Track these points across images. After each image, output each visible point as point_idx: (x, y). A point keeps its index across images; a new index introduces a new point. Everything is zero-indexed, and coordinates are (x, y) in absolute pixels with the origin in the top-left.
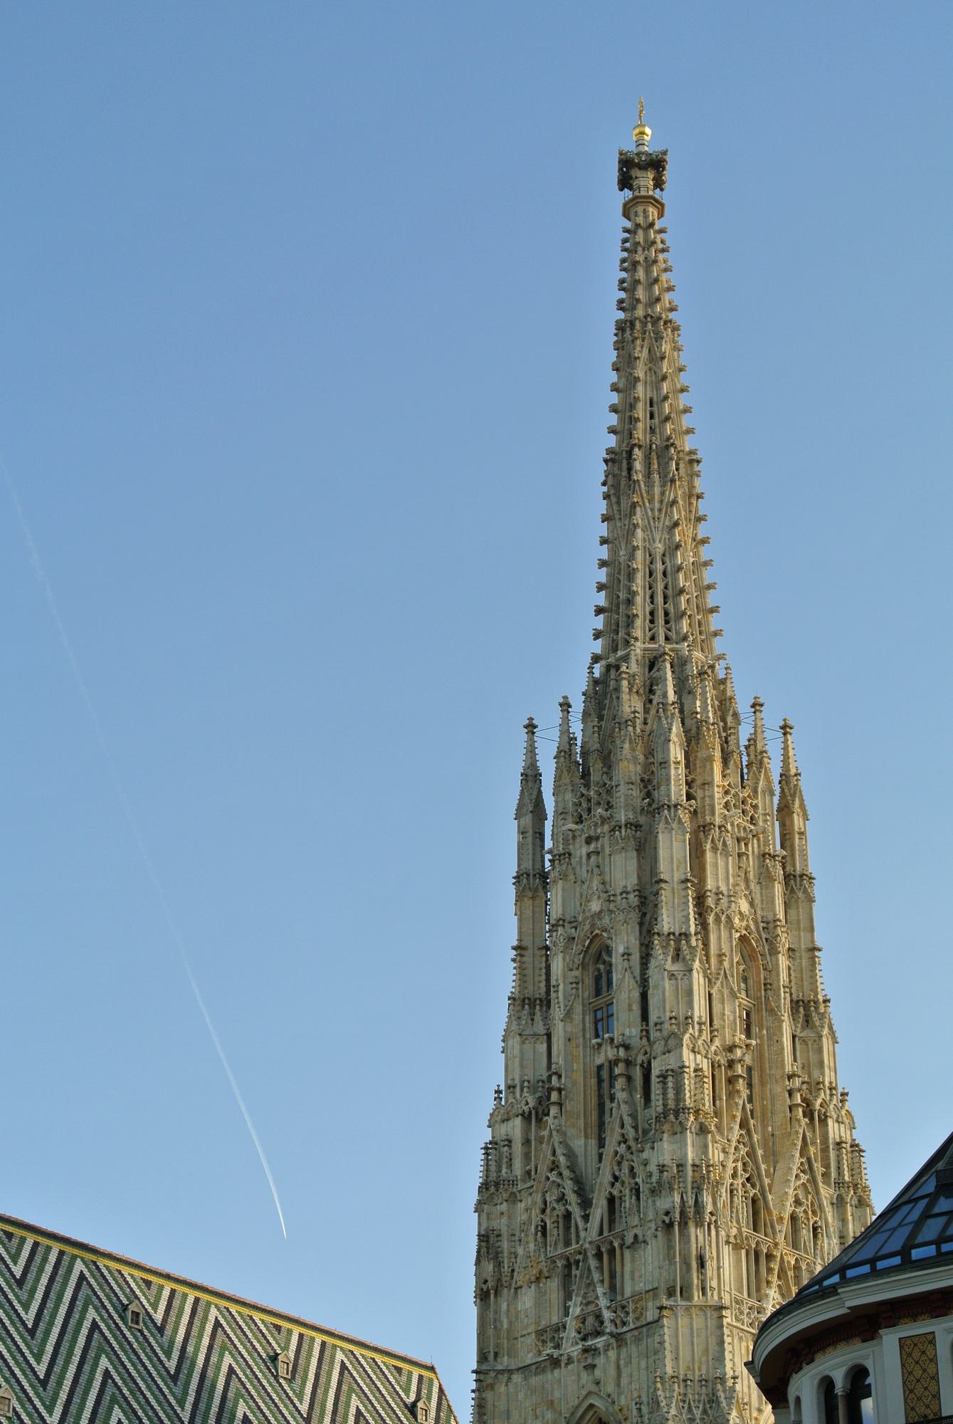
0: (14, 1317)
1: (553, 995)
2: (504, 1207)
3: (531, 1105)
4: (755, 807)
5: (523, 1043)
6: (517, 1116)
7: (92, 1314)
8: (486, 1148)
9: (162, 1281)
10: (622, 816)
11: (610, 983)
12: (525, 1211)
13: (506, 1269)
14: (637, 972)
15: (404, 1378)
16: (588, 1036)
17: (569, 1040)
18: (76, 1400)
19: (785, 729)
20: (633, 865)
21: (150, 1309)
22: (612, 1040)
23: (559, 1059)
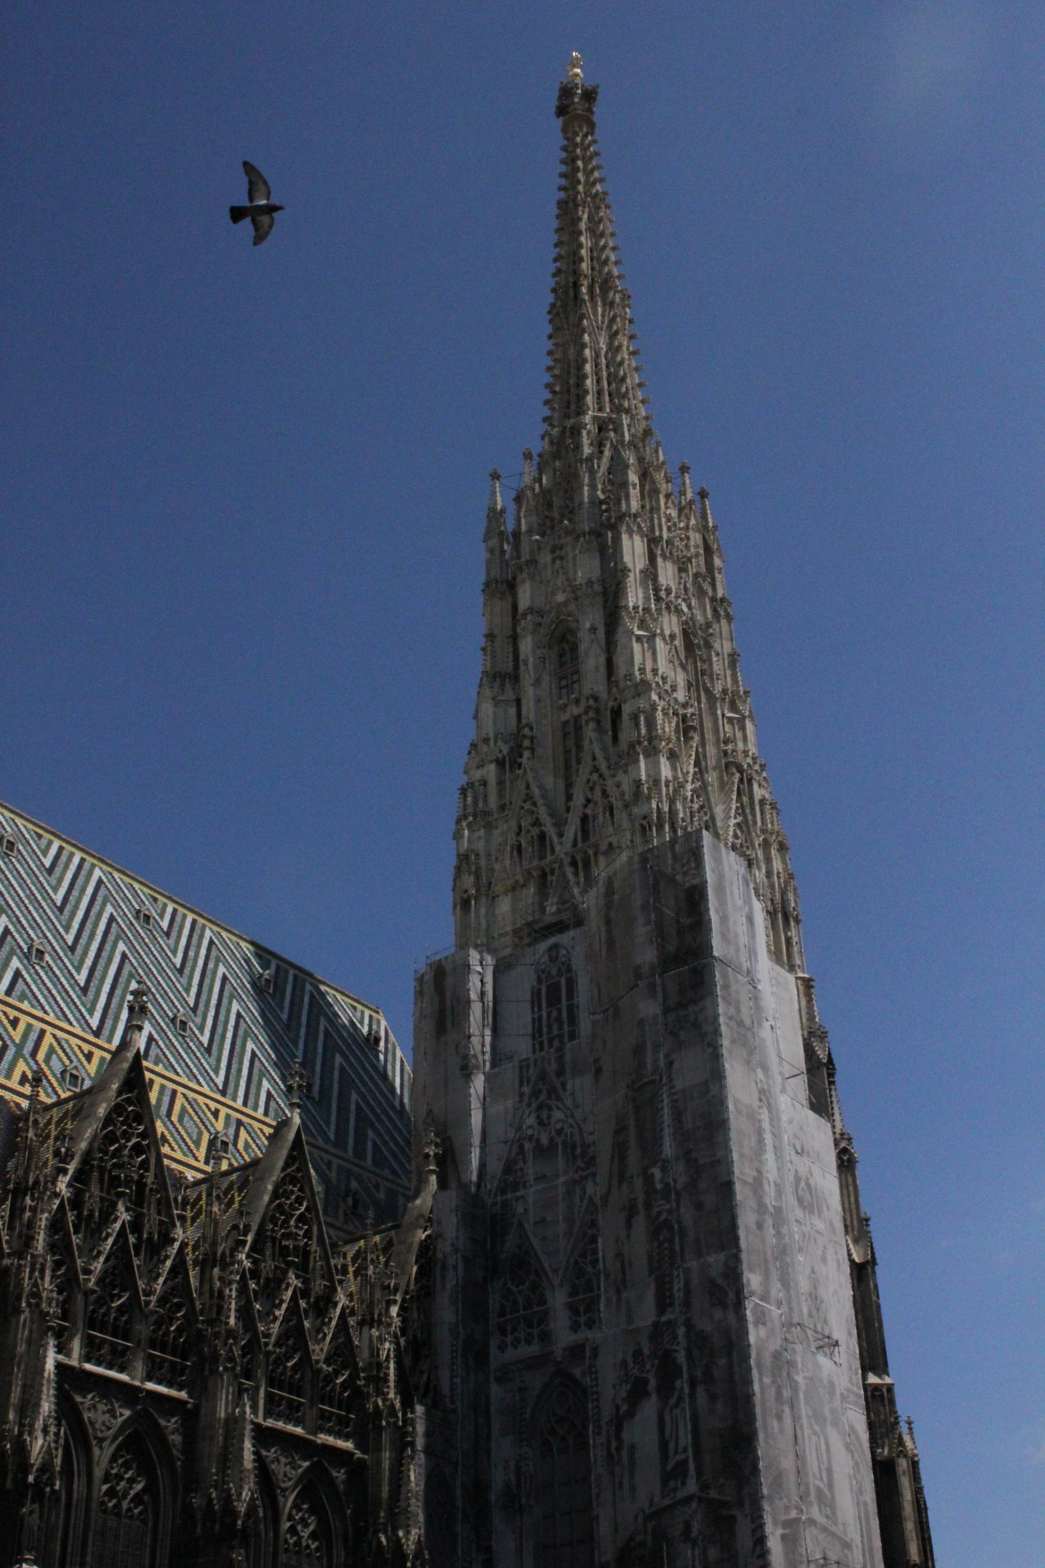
0: (45, 895)
1: (522, 668)
2: (482, 832)
3: (505, 750)
4: (688, 538)
5: (496, 706)
6: (492, 762)
7: (109, 909)
8: (463, 791)
9: (165, 900)
11: (575, 659)
12: (503, 833)
14: (603, 642)
15: (359, 1014)
17: (539, 701)
18: (100, 968)
20: (597, 562)
21: (157, 918)
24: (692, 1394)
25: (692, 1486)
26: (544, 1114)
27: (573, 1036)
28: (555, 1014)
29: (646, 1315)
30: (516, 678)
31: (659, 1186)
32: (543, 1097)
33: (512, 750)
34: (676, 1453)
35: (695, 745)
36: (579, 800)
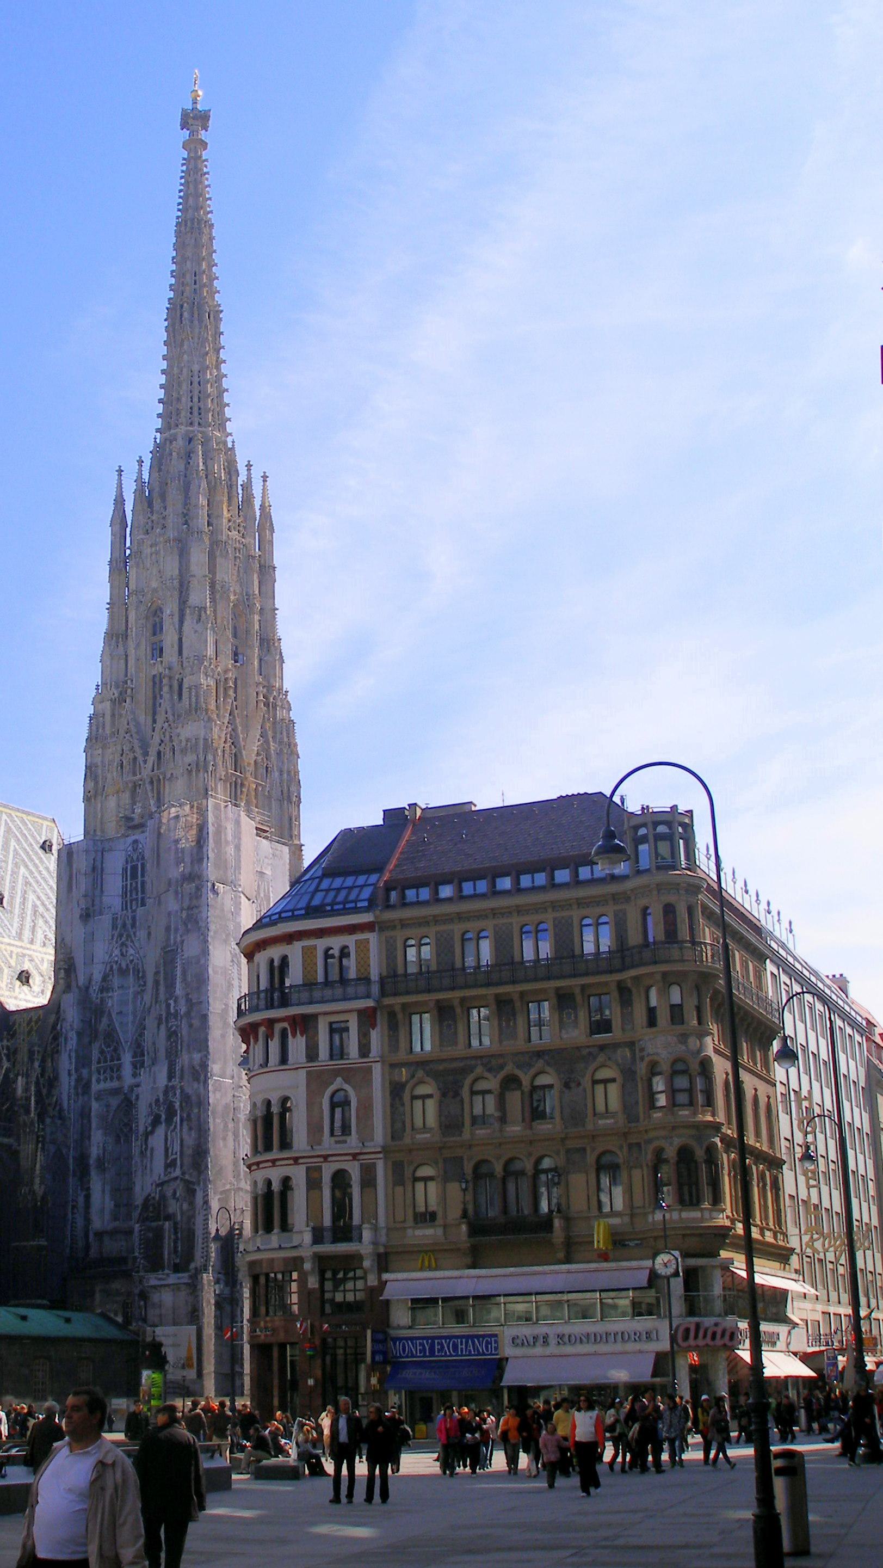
2: (100, 751)
8: (90, 717)
10: (171, 534)
12: (112, 754)
13: (100, 785)
16: (148, 657)
19: (265, 478)
20: (176, 564)
22: (162, 662)
23: (132, 669)
24: (181, 1125)
25: (178, 1172)
26: (124, 951)
27: (143, 904)
28: (134, 885)
29: (162, 1080)
30: (127, 639)
31: (172, 1011)
32: (123, 939)
33: (121, 693)
34: (172, 1154)
35: (231, 701)
36: (157, 739)
